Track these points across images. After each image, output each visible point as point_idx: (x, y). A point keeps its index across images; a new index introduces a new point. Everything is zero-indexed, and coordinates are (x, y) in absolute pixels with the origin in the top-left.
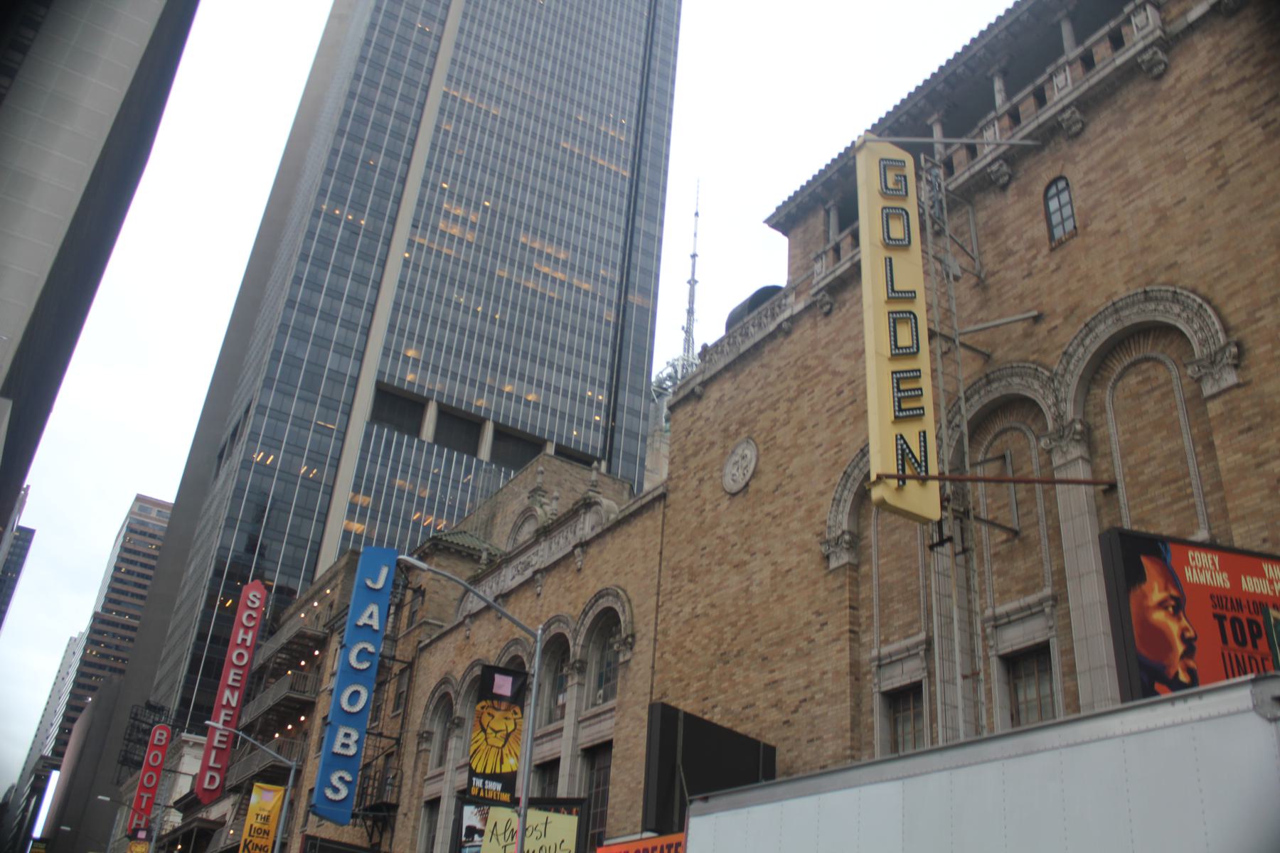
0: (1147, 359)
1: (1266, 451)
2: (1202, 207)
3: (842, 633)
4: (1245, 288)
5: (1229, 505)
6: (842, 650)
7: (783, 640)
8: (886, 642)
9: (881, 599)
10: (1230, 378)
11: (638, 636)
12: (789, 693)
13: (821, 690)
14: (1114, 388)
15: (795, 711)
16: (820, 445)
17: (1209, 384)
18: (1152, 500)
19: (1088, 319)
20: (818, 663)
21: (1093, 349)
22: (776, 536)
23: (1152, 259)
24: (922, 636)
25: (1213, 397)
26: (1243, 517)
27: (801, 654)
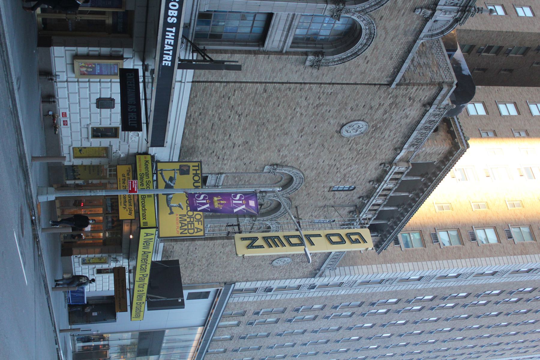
11: (315, 71)
12: (225, 153)
16: (323, 162)
22: (300, 146)
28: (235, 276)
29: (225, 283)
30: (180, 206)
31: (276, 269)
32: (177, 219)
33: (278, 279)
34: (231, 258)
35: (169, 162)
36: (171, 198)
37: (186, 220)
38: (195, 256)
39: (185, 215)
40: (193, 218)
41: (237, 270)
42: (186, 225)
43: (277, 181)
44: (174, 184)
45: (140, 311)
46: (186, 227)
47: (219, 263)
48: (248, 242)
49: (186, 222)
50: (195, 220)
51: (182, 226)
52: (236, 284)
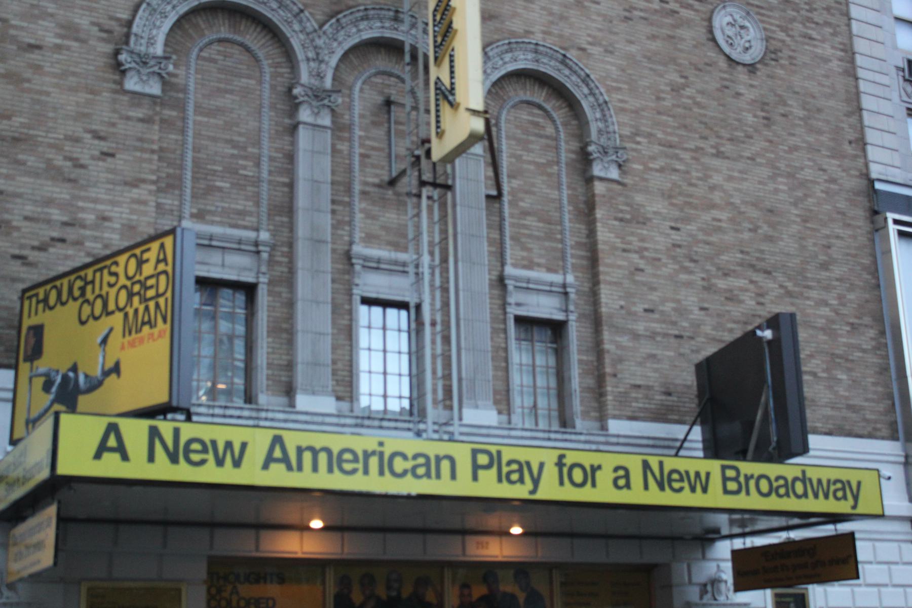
0: (540, 107)
1: (630, 243)
2: (611, 22)
3: (144, 181)
4: (633, 112)
5: (601, 269)
6: (144, 203)
7: (16, 140)
8: (199, 216)
9: (195, 161)
10: (614, 174)
12: (26, 218)
13: (95, 239)
14: (509, 111)
15: (42, 248)
17: (600, 167)
18: (525, 226)
19: (513, 40)
20: (96, 201)
21: (511, 67)
23: (567, 32)
24: (264, 236)
25: (601, 179)
26: (610, 283)
27: (53, 173)
28: (833, 181)
29: (876, 213)
30: (104, 341)
31: (786, 52)
32: (132, 345)
33: (851, 45)
34: (717, 197)
35: (14, 401)
36: (86, 376)
37: (136, 311)
38: (696, 314)
39: (126, 315)
40: (133, 284)
41: (790, 176)
42: (147, 309)
43: (245, 57)
44: (57, 371)
45: (804, 479)
46: (152, 304)
47: (746, 235)
48: (445, 109)
49: (141, 308)
50: (137, 278)
51: (149, 322)
52: (874, 175)
